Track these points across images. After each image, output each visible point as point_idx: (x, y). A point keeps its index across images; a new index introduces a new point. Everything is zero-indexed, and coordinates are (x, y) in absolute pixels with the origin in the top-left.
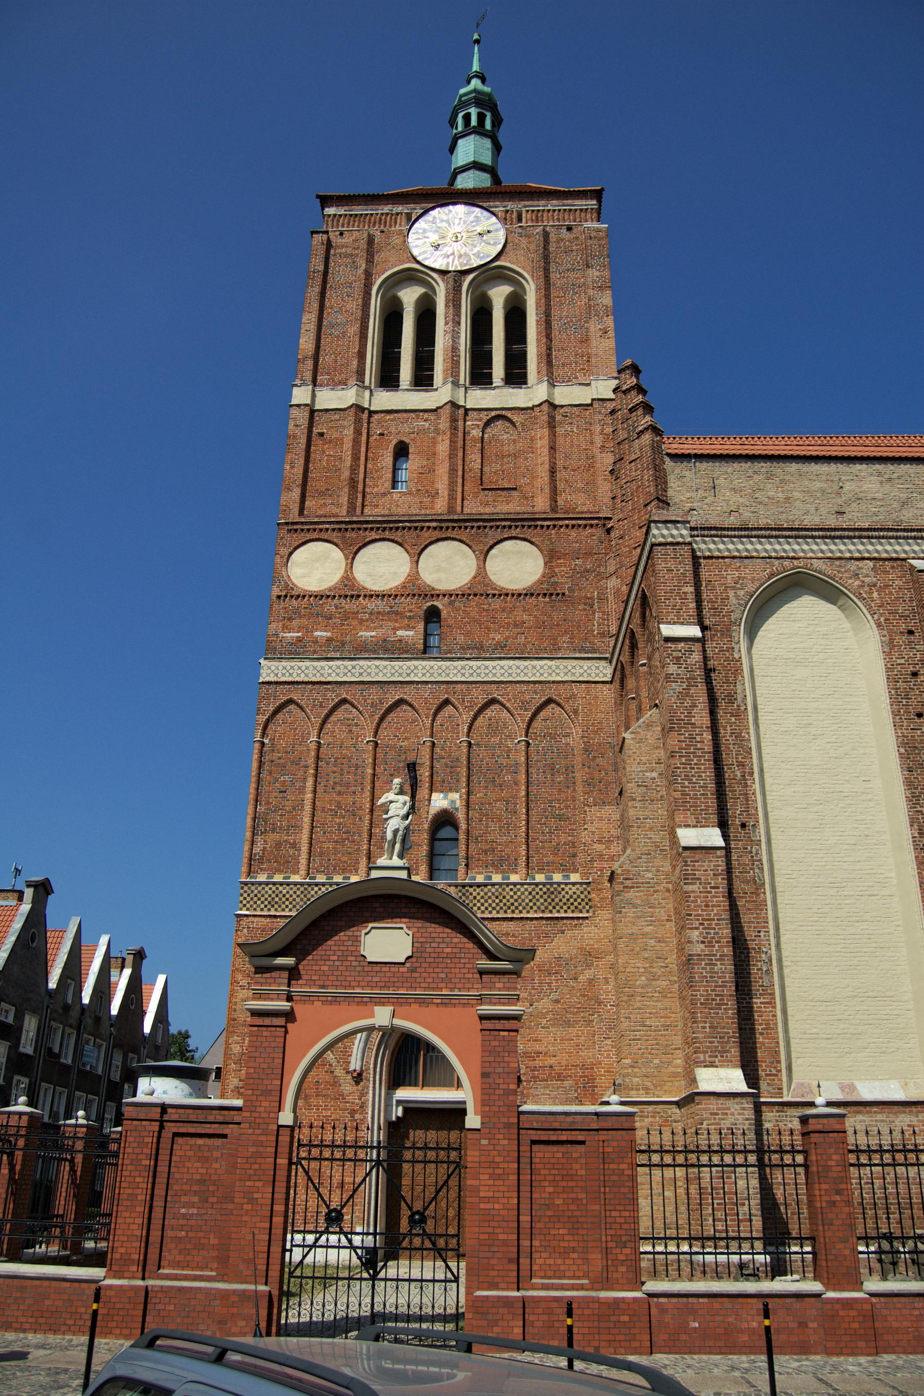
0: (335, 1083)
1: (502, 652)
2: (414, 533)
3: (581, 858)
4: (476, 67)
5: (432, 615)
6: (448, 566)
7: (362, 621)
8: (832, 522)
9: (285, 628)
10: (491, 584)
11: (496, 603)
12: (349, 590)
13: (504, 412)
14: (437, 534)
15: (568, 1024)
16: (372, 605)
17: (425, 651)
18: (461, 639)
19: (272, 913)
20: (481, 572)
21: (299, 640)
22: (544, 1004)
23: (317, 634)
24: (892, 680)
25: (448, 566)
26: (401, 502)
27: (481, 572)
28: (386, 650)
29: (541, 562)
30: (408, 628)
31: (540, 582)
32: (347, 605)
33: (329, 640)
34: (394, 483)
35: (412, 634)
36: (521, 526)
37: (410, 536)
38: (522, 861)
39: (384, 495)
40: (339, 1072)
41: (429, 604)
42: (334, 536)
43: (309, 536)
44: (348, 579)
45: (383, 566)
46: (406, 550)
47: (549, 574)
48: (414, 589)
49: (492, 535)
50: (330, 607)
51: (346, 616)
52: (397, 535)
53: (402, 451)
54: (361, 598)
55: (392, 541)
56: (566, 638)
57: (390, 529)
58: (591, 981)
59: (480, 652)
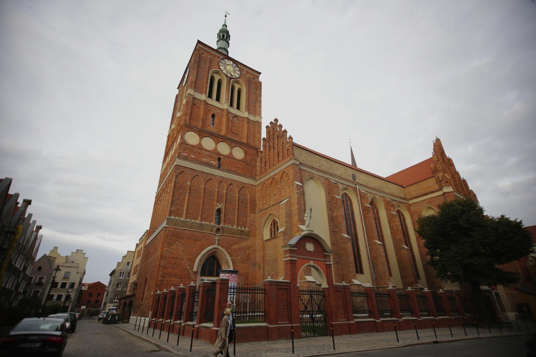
0: (189, 275)
1: (235, 173)
2: (217, 138)
3: (248, 225)
5: (219, 159)
6: (224, 149)
8: (319, 168)
9: (183, 152)
10: (233, 156)
11: (234, 161)
12: (200, 147)
14: (221, 140)
15: (244, 263)
16: (206, 153)
17: (219, 167)
18: (226, 167)
20: (231, 153)
22: (239, 258)
24: (327, 202)
25: (224, 149)
26: (212, 129)
27: (231, 153)
28: (209, 165)
29: (243, 154)
30: (214, 161)
31: (243, 159)
32: (200, 151)
33: (195, 158)
35: (215, 163)
36: (239, 144)
37: (216, 138)
38: (236, 223)
40: (190, 271)
43: (191, 130)
44: (200, 144)
45: (208, 144)
48: (215, 151)
49: (233, 144)
50: (195, 150)
51: (199, 153)
53: (213, 116)
57: (211, 135)
58: (249, 253)
59: (229, 171)
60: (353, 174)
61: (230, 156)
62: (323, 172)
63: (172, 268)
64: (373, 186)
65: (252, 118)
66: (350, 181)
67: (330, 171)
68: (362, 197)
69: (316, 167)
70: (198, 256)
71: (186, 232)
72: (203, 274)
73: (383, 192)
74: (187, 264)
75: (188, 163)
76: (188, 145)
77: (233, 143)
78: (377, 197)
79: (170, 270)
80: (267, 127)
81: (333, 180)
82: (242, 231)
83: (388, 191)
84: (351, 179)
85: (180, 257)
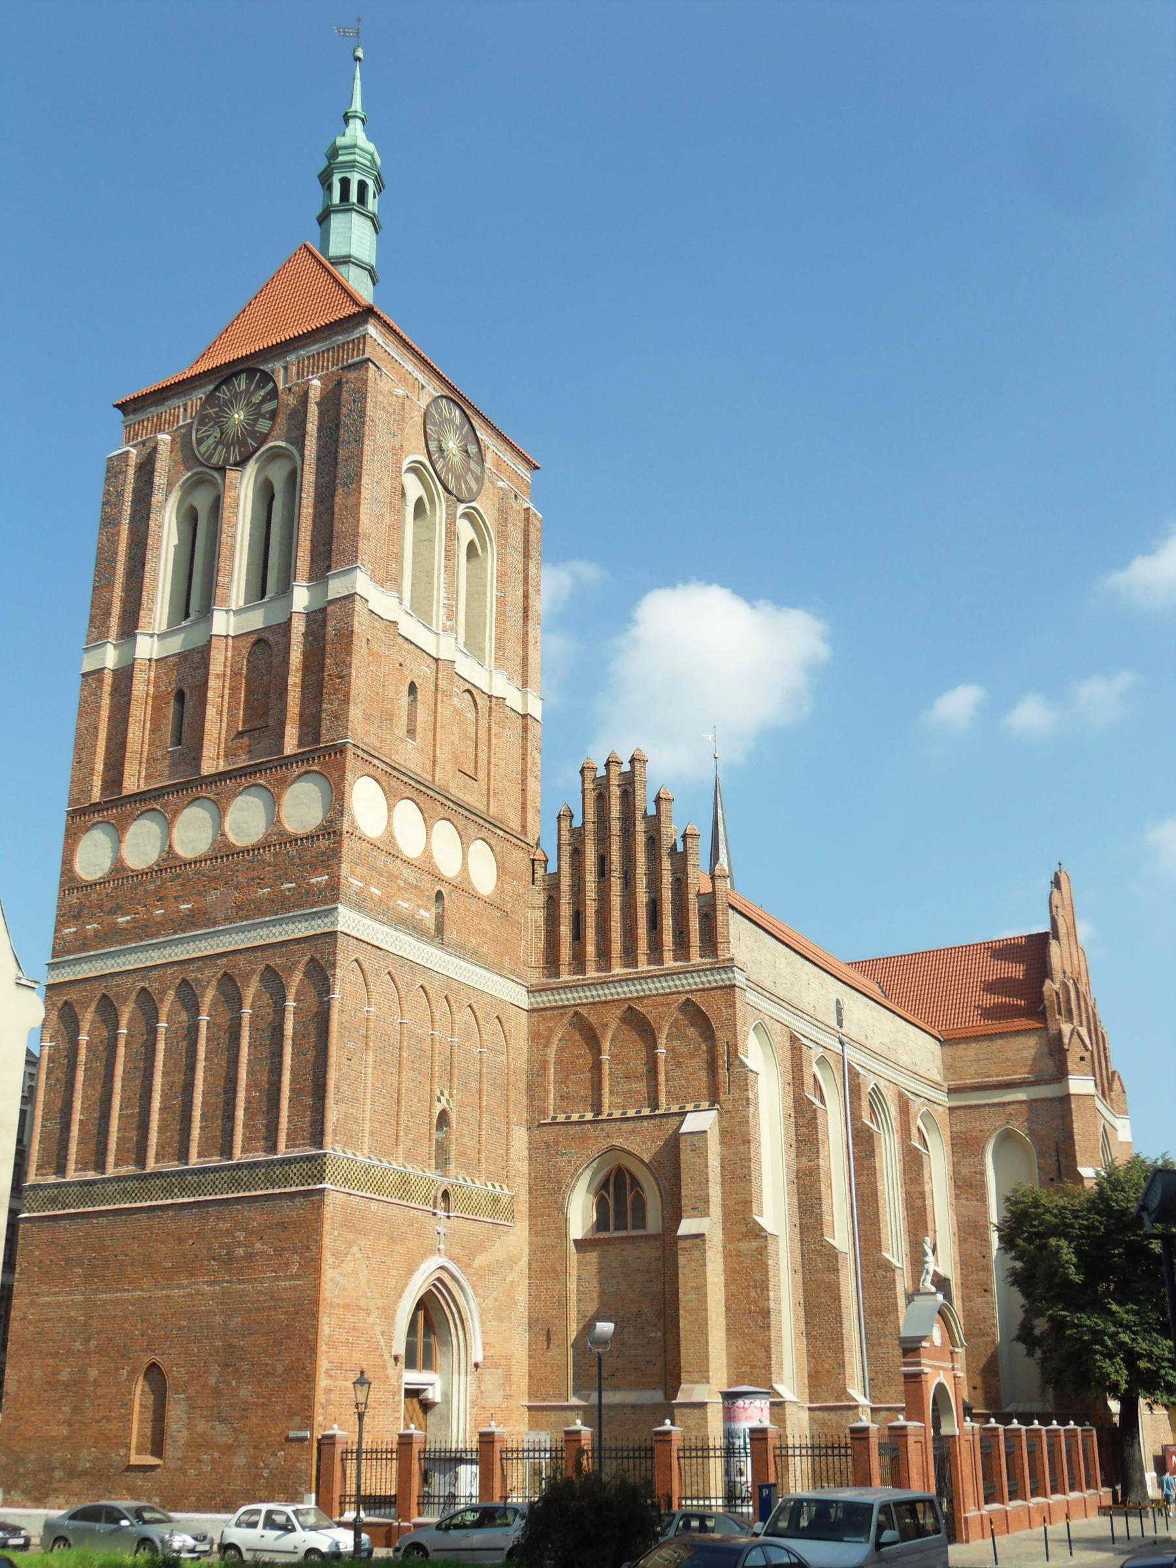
4: (357, 105)
7: (400, 889)
10: (470, 883)
13: (473, 690)
16: (407, 873)
19: (347, 1190)
21: (362, 890)
23: (373, 889)
34: (411, 732)
39: (402, 741)
41: (438, 888)
42: (383, 778)
46: (424, 819)
47: (499, 888)
52: (421, 799)
54: (398, 861)
55: (417, 804)
56: (507, 958)
58: (512, 1283)
60: (838, 1002)
61: (463, 887)
62: (780, 1001)
63: (346, 1343)
64: (874, 1043)
66: (825, 1028)
67: (792, 996)
68: (855, 1090)
69: (768, 984)
71: (373, 1206)
72: (411, 1363)
73: (896, 1065)
74: (378, 1329)
75: (368, 921)
78: (882, 1084)
79: (343, 1351)
81: (800, 1026)
82: (496, 1200)
83: (905, 1060)
84: (834, 1024)
85: (363, 1303)
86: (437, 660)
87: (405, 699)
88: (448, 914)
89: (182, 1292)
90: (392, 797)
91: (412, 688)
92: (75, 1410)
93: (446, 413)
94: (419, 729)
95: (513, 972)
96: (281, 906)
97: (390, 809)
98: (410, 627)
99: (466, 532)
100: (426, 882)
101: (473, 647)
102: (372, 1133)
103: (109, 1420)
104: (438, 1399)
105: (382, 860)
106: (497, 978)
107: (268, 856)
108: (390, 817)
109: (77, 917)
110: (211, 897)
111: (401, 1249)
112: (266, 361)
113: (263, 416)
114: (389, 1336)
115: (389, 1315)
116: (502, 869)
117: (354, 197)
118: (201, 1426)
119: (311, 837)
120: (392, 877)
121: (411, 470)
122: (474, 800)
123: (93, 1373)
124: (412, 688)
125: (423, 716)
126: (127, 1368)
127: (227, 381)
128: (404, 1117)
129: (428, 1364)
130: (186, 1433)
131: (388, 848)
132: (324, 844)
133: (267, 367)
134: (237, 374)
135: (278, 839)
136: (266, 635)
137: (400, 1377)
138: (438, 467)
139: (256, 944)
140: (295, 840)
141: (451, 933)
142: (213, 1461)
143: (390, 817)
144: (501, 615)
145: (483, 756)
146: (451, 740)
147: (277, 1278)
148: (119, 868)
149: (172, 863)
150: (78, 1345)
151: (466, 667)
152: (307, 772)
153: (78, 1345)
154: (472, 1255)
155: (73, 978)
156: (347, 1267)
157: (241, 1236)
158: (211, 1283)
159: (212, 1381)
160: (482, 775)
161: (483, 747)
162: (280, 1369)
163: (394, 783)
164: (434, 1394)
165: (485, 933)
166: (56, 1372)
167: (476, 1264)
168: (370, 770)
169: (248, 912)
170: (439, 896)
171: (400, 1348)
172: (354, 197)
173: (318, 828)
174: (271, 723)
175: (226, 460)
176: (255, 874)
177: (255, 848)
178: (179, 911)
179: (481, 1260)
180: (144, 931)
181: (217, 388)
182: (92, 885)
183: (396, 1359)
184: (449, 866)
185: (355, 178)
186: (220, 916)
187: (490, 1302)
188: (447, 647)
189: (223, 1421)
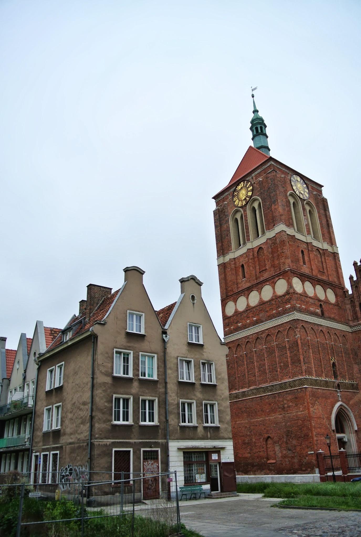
10: (328, 300)
16: (311, 301)
34: (304, 263)
35: (318, 311)
47: (337, 301)
52: (311, 281)
61: (327, 302)
63: (319, 428)
65: (330, 249)
70: (331, 414)
71: (319, 390)
72: (338, 432)
74: (327, 423)
76: (297, 294)
77: (325, 284)
79: (319, 430)
80: (355, 264)
82: (353, 385)
85: (321, 416)
86: (307, 243)
87: (301, 255)
88: (324, 309)
89: (273, 417)
90: (303, 282)
91: (302, 252)
92: (251, 449)
93: (296, 178)
94: (306, 262)
95: (345, 322)
96: (279, 314)
97: (303, 284)
98: (298, 236)
99: (308, 208)
100: (317, 302)
101: (316, 237)
102: (315, 371)
103: (260, 452)
104: (347, 441)
105: (303, 298)
106: (341, 325)
107: (273, 302)
108: (303, 287)
109: (228, 325)
110: (261, 315)
111: (329, 401)
112: (247, 178)
113: (249, 191)
114: (330, 424)
115: (329, 419)
116: (336, 295)
117: (260, 131)
118: (284, 452)
119: (284, 295)
120: (307, 302)
121: (290, 195)
122: (324, 278)
123: (254, 440)
124: (302, 252)
125: (306, 258)
126: (262, 438)
127: (238, 185)
128: (323, 366)
129: (343, 432)
130: (280, 454)
131: (304, 294)
132: (287, 297)
133: (247, 179)
134: (240, 183)
135: (275, 298)
136: (261, 246)
137: (335, 435)
138: (297, 193)
139: (275, 325)
140: (280, 297)
141: (326, 314)
142: (289, 461)
143: (303, 287)
144: (322, 227)
145: (325, 266)
146: (315, 264)
147: (297, 412)
148: (236, 312)
149: (249, 308)
150: (248, 433)
151: (315, 243)
152: (279, 279)
153: (248, 433)
154: (349, 401)
155: (230, 341)
156: (316, 407)
157: (285, 402)
158: (281, 414)
159: (285, 440)
160: (325, 271)
161: (324, 263)
162: (303, 436)
163: (303, 278)
164: (345, 439)
165: (335, 313)
166: (244, 440)
167: (350, 403)
168: (296, 275)
169: (270, 318)
170: (321, 305)
171: (334, 427)
172: (260, 131)
173: (285, 293)
174: (267, 268)
175: (242, 204)
176: (271, 307)
177: (270, 301)
178: (253, 320)
179: (351, 402)
180: (245, 327)
181: (236, 187)
182: (230, 317)
183: (333, 431)
184: (322, 297)
185: (259, 127)
186: (264, 320)
187: (356, 413)
188: (309, 239)
189: (290, 450)
